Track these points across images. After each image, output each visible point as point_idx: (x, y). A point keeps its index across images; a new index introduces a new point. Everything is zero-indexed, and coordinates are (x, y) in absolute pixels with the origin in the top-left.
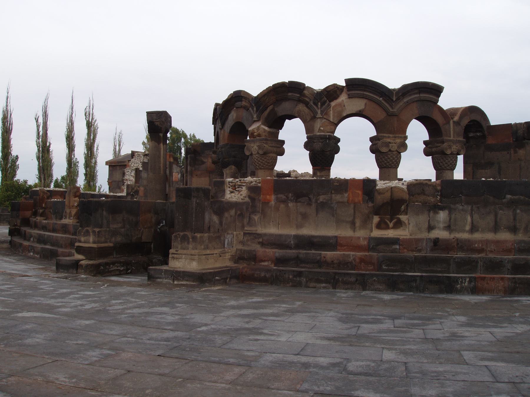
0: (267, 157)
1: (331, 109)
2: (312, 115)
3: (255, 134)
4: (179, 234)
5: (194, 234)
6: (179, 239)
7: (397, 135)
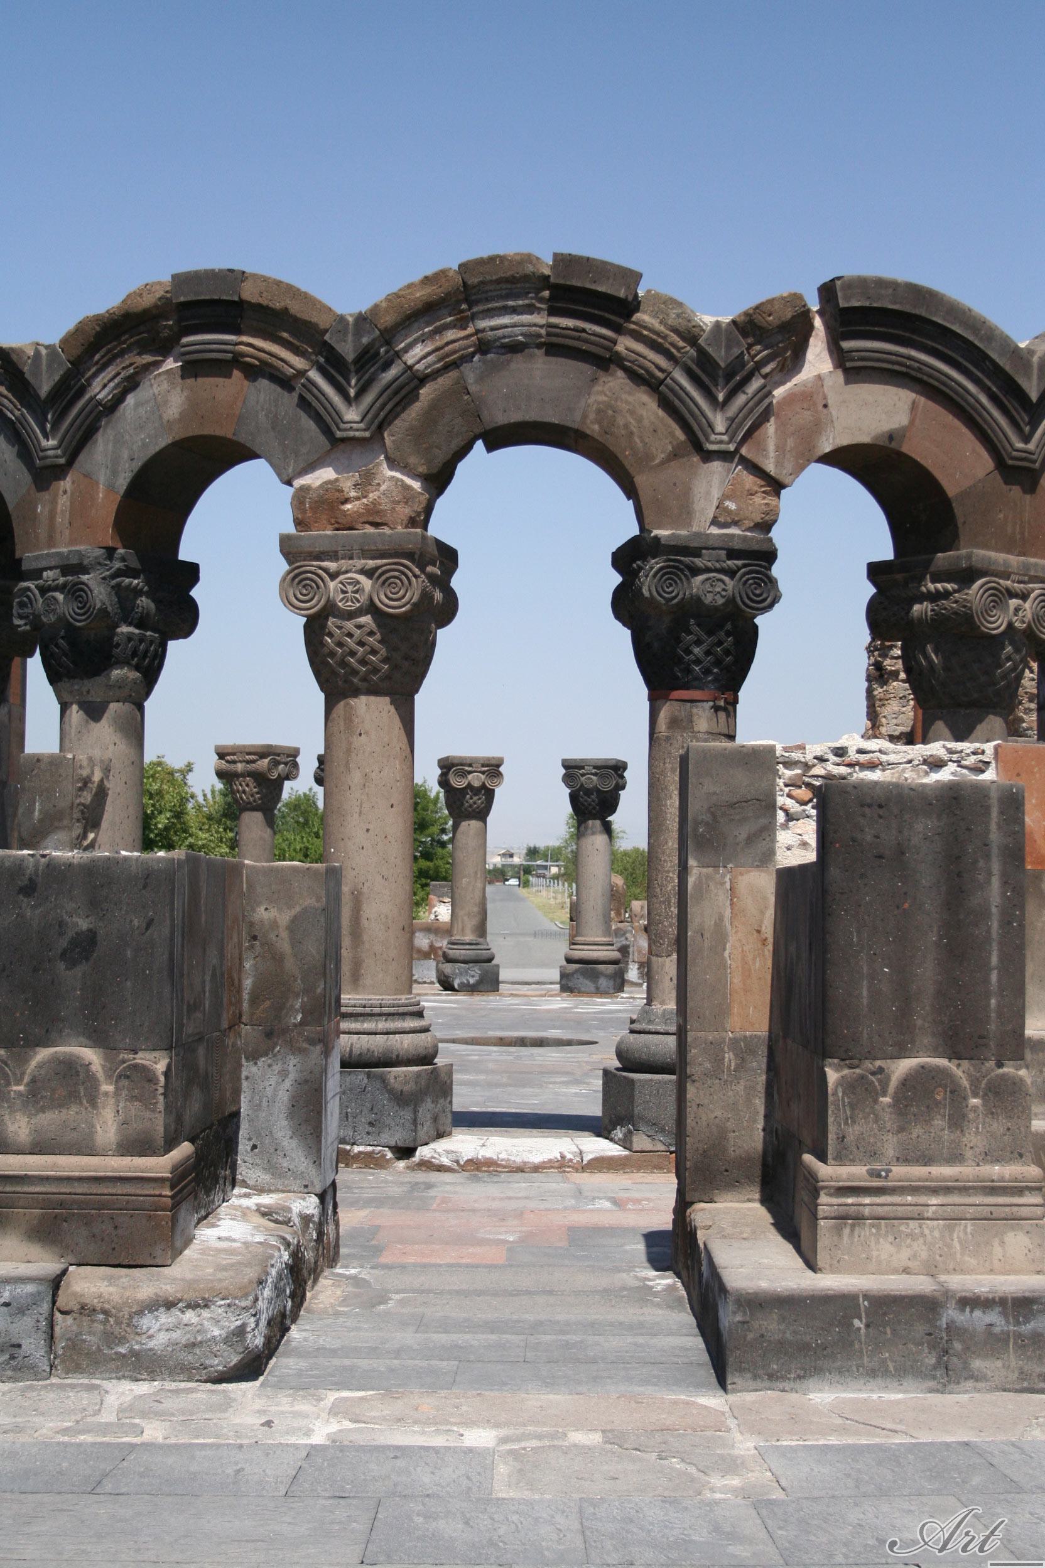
2: (680, 435)
3: (348, 506)
4: (881, 1070)
5: (1000, 1065)
6: (887, 1100)
7: (1032, 560)
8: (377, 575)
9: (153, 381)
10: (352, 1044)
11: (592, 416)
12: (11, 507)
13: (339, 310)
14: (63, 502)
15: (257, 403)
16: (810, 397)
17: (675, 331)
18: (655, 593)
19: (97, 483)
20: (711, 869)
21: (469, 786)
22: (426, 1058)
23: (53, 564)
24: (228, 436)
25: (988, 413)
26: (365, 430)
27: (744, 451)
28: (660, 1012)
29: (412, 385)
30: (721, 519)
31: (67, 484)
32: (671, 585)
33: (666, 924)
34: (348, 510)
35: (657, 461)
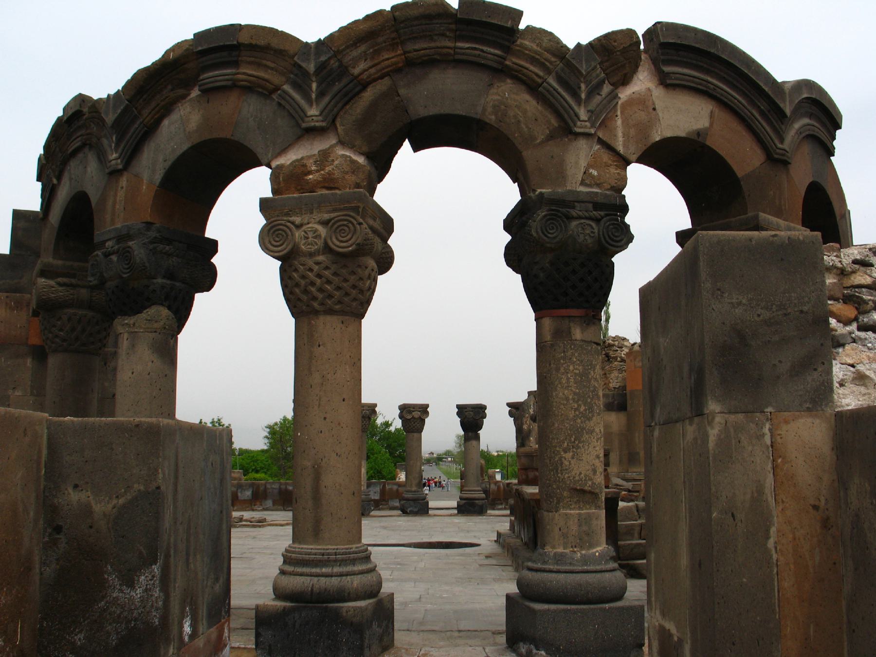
0: (359, 266)
1: (619, 113)
2: (554, 122)
3: (311, 177)
8: (331, 224)
10: (313, 585)
11: (490, 110)
12: (93, 205)
13: (304, 39)
14: (121, 194)
16: (642, 102)
18: (541, 234)
19: (143, 180)
20: (741, 416)
21: (413, 417)
22: (373, 591)
23: (112, 236)
25: (760, 123)
26: (322, 121)
27: (600, 134)
28: (552, 554)
29: (357, 89)
30: (587, 182)
31: (124, 181)
32: (553, 228)
33: (554, 486)
34: (310, 179)
35: (538, 141)
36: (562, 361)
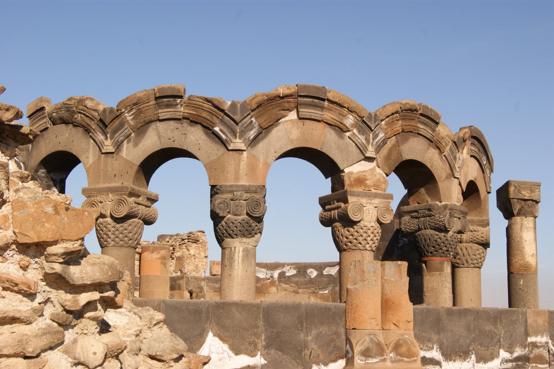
2: (448, 170)
3: (367, 182)
9: (284, 123)
11: (428, 161)
15: (331, 138)
17: (447, 136)
23: (240, 190)
24: (319, 149)
35: (443, 179)
36: (444, 282)
